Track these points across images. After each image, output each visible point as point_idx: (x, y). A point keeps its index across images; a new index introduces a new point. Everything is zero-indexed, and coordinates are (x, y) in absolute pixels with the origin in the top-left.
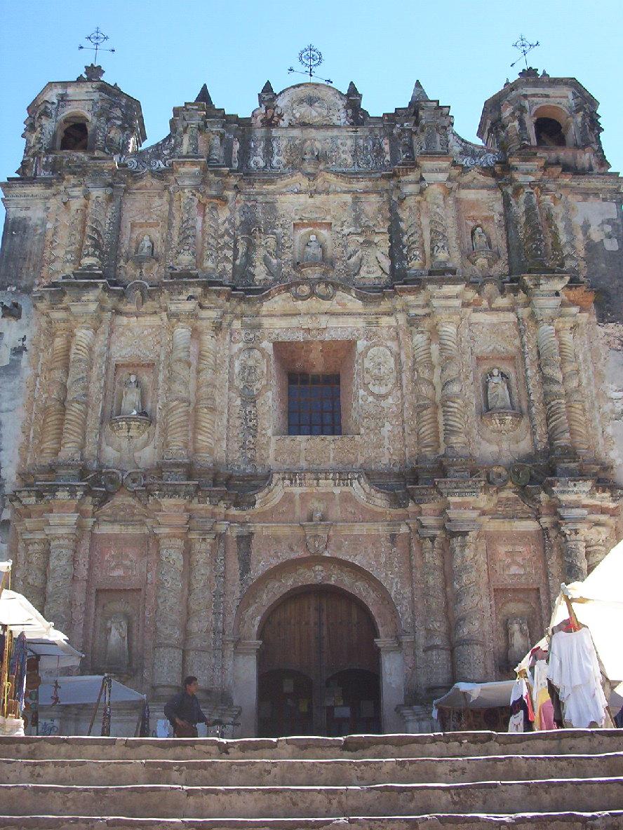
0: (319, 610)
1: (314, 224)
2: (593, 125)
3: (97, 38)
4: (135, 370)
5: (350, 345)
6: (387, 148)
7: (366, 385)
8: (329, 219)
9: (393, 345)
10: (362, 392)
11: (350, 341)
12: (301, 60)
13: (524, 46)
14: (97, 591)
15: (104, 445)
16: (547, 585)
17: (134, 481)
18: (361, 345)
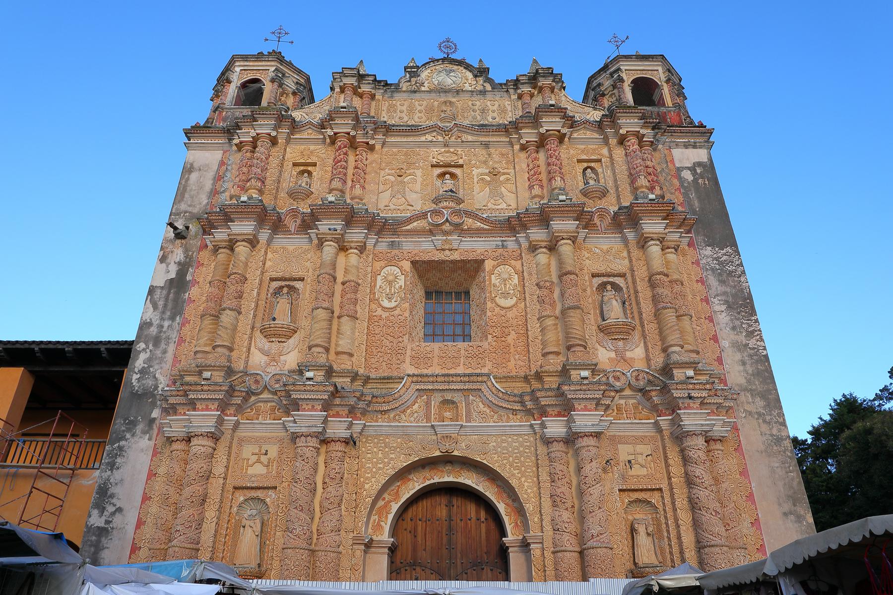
0: (449, 505)
1: (450, 166)
2: (679, 92)
3: (280, 34)
4: (287, 283)
5: (478, 264)
6: (509, 108)
7: (493, 300)
8: (461, 162)
9: (518, 264)
10: (489, 305)
11: (476, 261)
12: (440, 49)
13: (617, 42)
14: (235, 488)
15: (252, 349)
16: (670, 484)
17: (278, 381)
18: (488, 264)
